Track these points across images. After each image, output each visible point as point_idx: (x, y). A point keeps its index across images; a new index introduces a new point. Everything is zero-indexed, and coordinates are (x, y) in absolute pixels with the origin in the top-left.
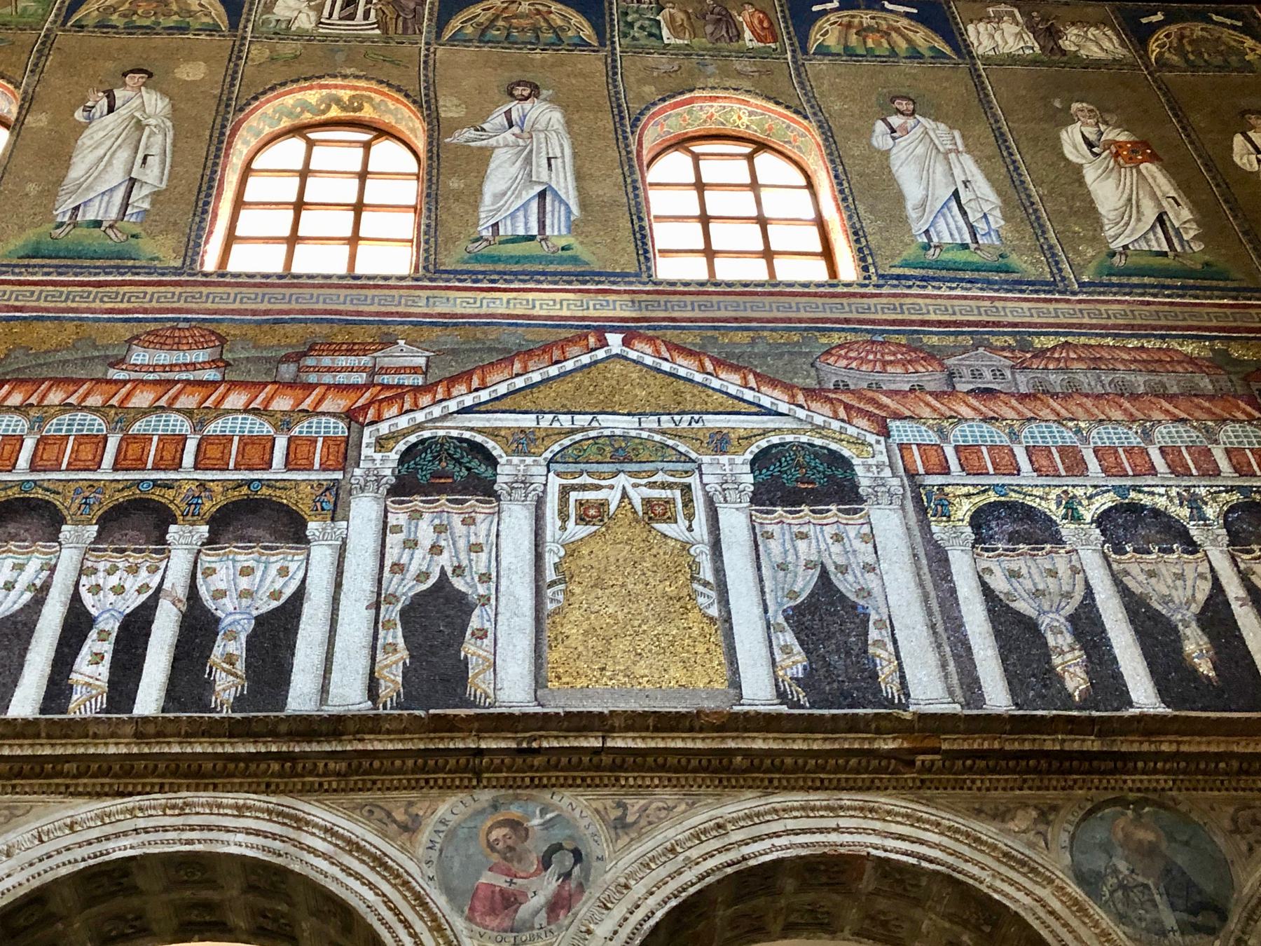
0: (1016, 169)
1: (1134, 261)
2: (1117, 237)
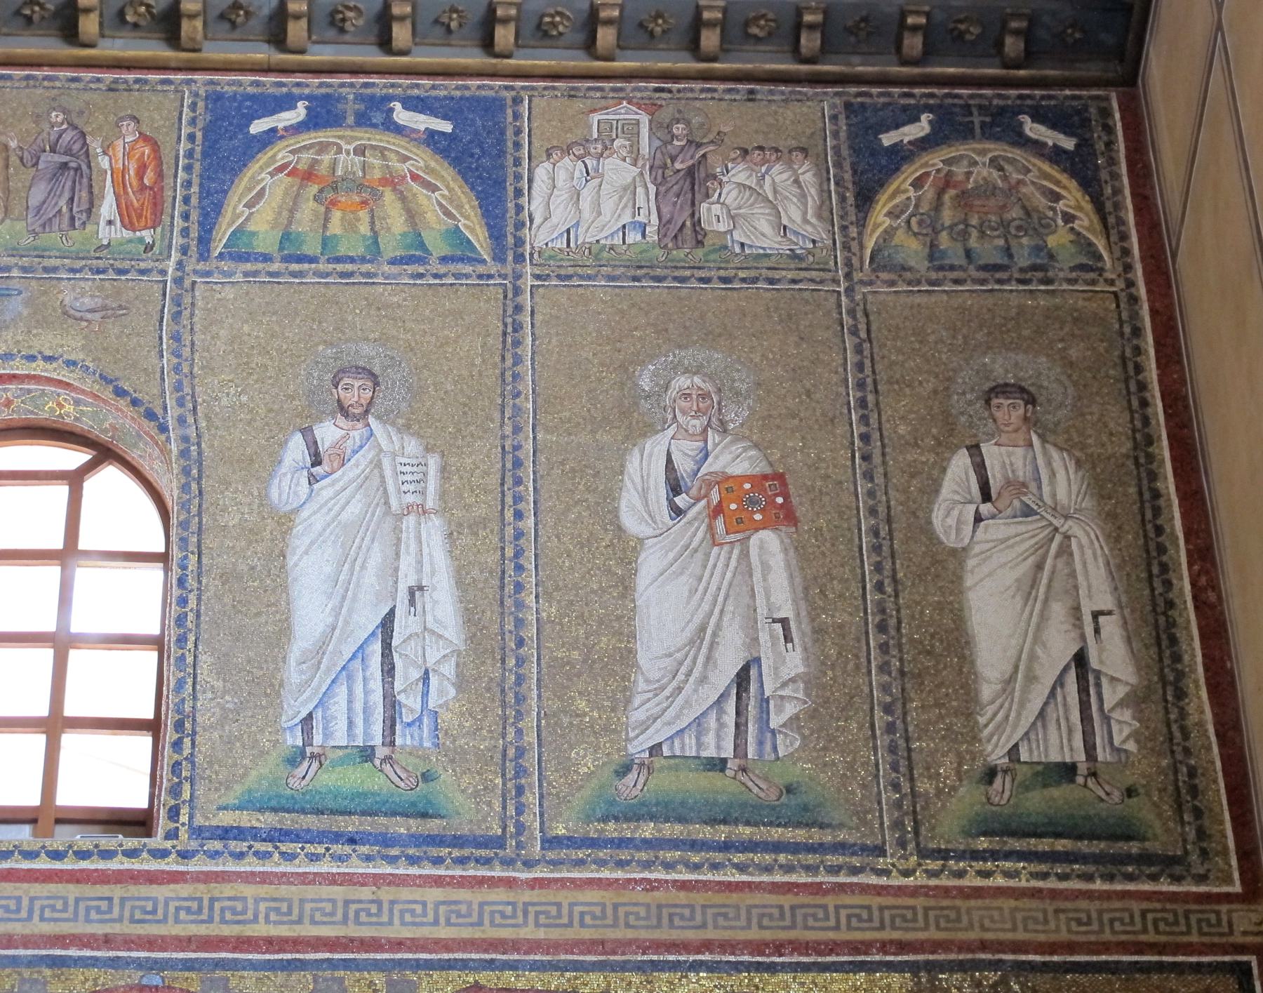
0: (518, 554)
1: (664, 783)
2: (644, 726)
